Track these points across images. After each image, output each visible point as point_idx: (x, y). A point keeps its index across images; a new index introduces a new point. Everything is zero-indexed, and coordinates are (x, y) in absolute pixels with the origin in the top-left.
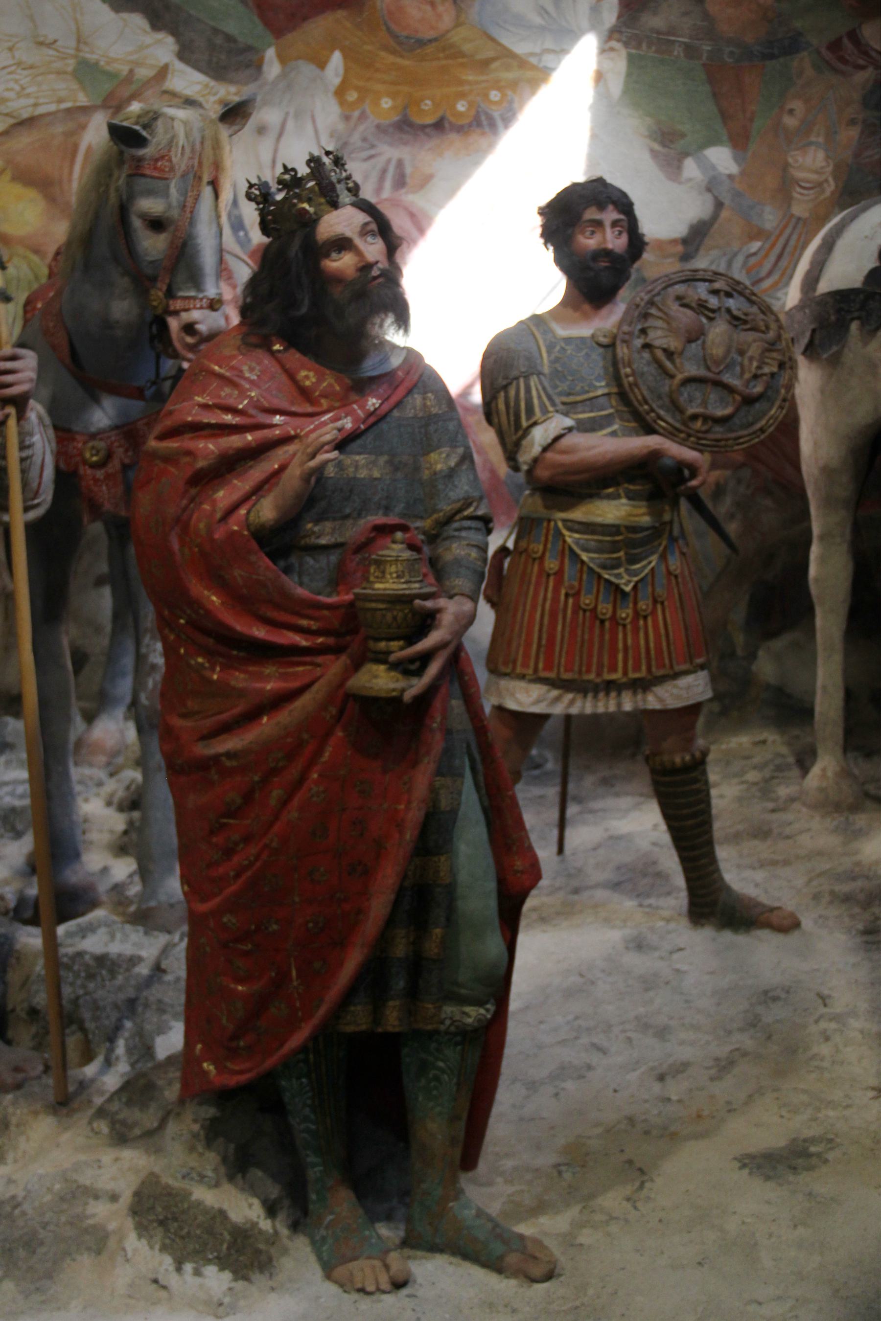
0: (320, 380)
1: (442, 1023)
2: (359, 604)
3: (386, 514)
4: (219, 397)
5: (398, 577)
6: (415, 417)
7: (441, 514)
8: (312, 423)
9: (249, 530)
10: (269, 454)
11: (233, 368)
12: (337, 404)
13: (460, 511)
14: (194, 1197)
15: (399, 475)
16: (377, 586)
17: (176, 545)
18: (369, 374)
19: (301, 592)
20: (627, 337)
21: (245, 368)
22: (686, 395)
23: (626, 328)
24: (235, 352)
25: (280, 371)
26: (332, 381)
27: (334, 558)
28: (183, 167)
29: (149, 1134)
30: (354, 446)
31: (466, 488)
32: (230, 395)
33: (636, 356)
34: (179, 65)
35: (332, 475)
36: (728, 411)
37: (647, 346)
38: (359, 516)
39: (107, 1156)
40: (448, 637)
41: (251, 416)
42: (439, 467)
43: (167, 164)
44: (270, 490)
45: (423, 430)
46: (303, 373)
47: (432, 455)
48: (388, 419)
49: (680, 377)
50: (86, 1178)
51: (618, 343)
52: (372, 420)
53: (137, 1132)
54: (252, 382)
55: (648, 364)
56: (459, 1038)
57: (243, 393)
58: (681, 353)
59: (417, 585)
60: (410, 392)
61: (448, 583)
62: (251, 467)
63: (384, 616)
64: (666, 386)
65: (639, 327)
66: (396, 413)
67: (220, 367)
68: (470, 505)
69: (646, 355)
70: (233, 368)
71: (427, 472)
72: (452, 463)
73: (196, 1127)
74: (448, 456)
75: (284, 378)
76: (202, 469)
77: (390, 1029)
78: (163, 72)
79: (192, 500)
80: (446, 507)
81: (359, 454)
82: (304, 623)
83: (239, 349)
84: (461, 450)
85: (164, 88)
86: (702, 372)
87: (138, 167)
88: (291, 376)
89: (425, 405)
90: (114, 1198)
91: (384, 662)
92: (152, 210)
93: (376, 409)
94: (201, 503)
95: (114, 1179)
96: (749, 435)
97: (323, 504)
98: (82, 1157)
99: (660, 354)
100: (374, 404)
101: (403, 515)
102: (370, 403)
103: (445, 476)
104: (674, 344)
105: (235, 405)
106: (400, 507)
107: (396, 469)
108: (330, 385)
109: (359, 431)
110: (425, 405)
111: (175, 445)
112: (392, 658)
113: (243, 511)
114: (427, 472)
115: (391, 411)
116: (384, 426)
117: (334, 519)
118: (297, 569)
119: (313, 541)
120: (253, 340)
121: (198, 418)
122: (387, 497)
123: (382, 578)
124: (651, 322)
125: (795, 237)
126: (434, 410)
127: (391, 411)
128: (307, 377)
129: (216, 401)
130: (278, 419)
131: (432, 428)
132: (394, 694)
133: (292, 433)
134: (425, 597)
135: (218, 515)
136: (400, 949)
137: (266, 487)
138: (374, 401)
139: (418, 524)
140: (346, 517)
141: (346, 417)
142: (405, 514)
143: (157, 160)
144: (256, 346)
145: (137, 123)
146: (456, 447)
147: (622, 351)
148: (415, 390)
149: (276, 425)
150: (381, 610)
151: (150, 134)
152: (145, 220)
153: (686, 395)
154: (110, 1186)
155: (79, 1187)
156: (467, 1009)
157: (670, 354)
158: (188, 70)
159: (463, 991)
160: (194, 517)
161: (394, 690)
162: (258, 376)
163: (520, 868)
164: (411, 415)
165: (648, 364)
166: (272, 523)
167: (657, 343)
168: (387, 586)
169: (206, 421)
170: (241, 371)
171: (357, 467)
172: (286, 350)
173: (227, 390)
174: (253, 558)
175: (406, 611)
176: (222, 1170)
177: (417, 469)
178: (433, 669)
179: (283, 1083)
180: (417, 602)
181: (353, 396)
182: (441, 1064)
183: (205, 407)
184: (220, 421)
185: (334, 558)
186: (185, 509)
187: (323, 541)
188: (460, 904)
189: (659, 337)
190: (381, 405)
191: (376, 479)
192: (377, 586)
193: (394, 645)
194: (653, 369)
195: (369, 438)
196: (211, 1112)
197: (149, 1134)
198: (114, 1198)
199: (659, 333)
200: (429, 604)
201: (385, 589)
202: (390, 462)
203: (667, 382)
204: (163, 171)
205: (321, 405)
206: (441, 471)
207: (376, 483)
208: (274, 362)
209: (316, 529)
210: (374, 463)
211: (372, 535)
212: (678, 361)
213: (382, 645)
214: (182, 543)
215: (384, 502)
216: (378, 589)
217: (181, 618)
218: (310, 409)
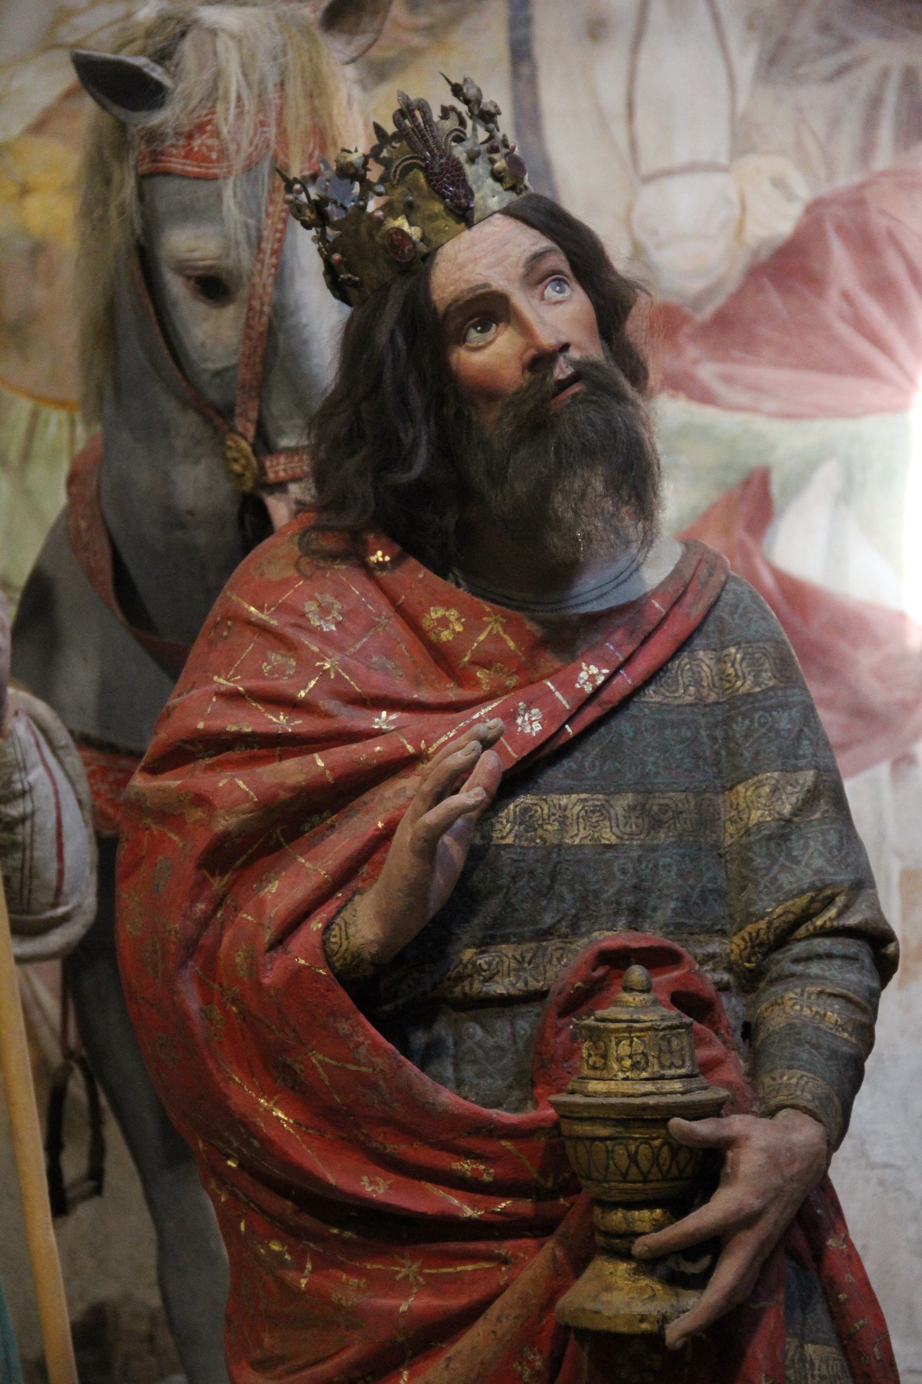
0: (471, 629)
2: (565, 1126)
3: (633, 926)
4: (259, 673)
5: (635, 1066)
6: (699, 703)
8: (454, 724)
9: (330, 965)
10: (366, 797)
11: (284, 609)
12: (511, 682)
13: (806, 916)
16: (594, 1086)
17: (193, 1003)
18: (583, 610)
19: (447, 1097)
21: (310, 607)
24: (291, 573)
25: (386, 610)
26: (498, 628)
27: (524, 1026)
28: (246, 149)
30: (556, 774)
32: (280, 670)
35: (509, 840)
38: (575, 929)
41: (326, 715)
42: (756, 815)
43: (211, 142)
44: (373, 878)
45: (719, 733)
46: (436, 613)
47: (740, 788)
48: (633, 710)
52: (591, 713)
54: (325, 638)
57: (307, 665)
59: (677, 1086)
60: (684, 645)
61: (767, 1081)
62: (332, 827)
63: (610, 1153)
66: (652, 695)
67: (260, 608)
68: (831, 900)
70: (284, 609)
71: (731, 829)
72: (787, 810)
74: (775, 790)
75: (395, 627)
76: (226, 835)
79: (219, 902)
81: (569, 791)
82: (465, 1167)
83: (297, 565)
84: (808, 777)
87: (155, 156)
89: (723, 676)
91: (627, 1256)
92: (197, 254)
93: (598, 690)
94: (237, 909)
97: (493, 905)
100: (592, 678)
101: (676, 928)
102: (583, 675)
103: (769, 838)
105: (291, 691)
107: (656, 824)
108: (495, 638)
109: (562, 741)
110: (723, 676)
111: (174, 783)
112: (639, 1246)
113: (316, 925)
114: (731, 829)
115: (638, 690)
116: (623, 725)
117: (521, 939)
118: (452, 1052)
119: (477, 987)
120: (329, 544)
121: (217, 724)
122: (635, 887)
123: (601, 1070)
126: (745, 686)
127: (638, 690)
128: (444, 622)
129: (253, 683)
131: (739, 727)
133: (410, 748)
134: (715, 1110)
135: (268, 936)
137: (365, 869)
138: (594, 670)
139: (714, 947)
140: (547, 934)
141: (528, 709)
142: (679, 926)
143: (190, 136)
144: (334, 557)
145: (142, 52)
146: (797, 769)
148: (698, 641)
149: (380, 733)
150: (603, 1139)
151: (173, 76)
152: (189, 278)
160: (226, 941)
162: (338, 624)
164: (689, 699)
166: (374, 949)
168: (612, 1086)
169: (232, 728)
170: (303, 615)
171: (563, 821)
172: (396, 562)
173: (276, 658)
174: (344, 1027)
175: (657, 1143)
180: (677, 1122)
181: (549, 661)
183: (232, 696)
184: (261, 729)
185: (524, 1026)
186: (206, 921)
187: (499, 988)
190: (609, 679)
191: (608, 847)
192: (594, 1086)
193: (643, 1217)
195: (592, 750)
200: (704, 1128)
201: (608, 1094)
202: (639, 809)
204: (207, 159)
205: (477, 683)
206: (759, 825)
207: (608, 855)
208: (373, 592)
209: (482, 961)
210: (602, 810)
211: (600, 972)
213: (617, 1217)
214: (207, 997)
215: (629, 899)
216: (595, 1094)
217: (228, 1157)
218: (453, 693)
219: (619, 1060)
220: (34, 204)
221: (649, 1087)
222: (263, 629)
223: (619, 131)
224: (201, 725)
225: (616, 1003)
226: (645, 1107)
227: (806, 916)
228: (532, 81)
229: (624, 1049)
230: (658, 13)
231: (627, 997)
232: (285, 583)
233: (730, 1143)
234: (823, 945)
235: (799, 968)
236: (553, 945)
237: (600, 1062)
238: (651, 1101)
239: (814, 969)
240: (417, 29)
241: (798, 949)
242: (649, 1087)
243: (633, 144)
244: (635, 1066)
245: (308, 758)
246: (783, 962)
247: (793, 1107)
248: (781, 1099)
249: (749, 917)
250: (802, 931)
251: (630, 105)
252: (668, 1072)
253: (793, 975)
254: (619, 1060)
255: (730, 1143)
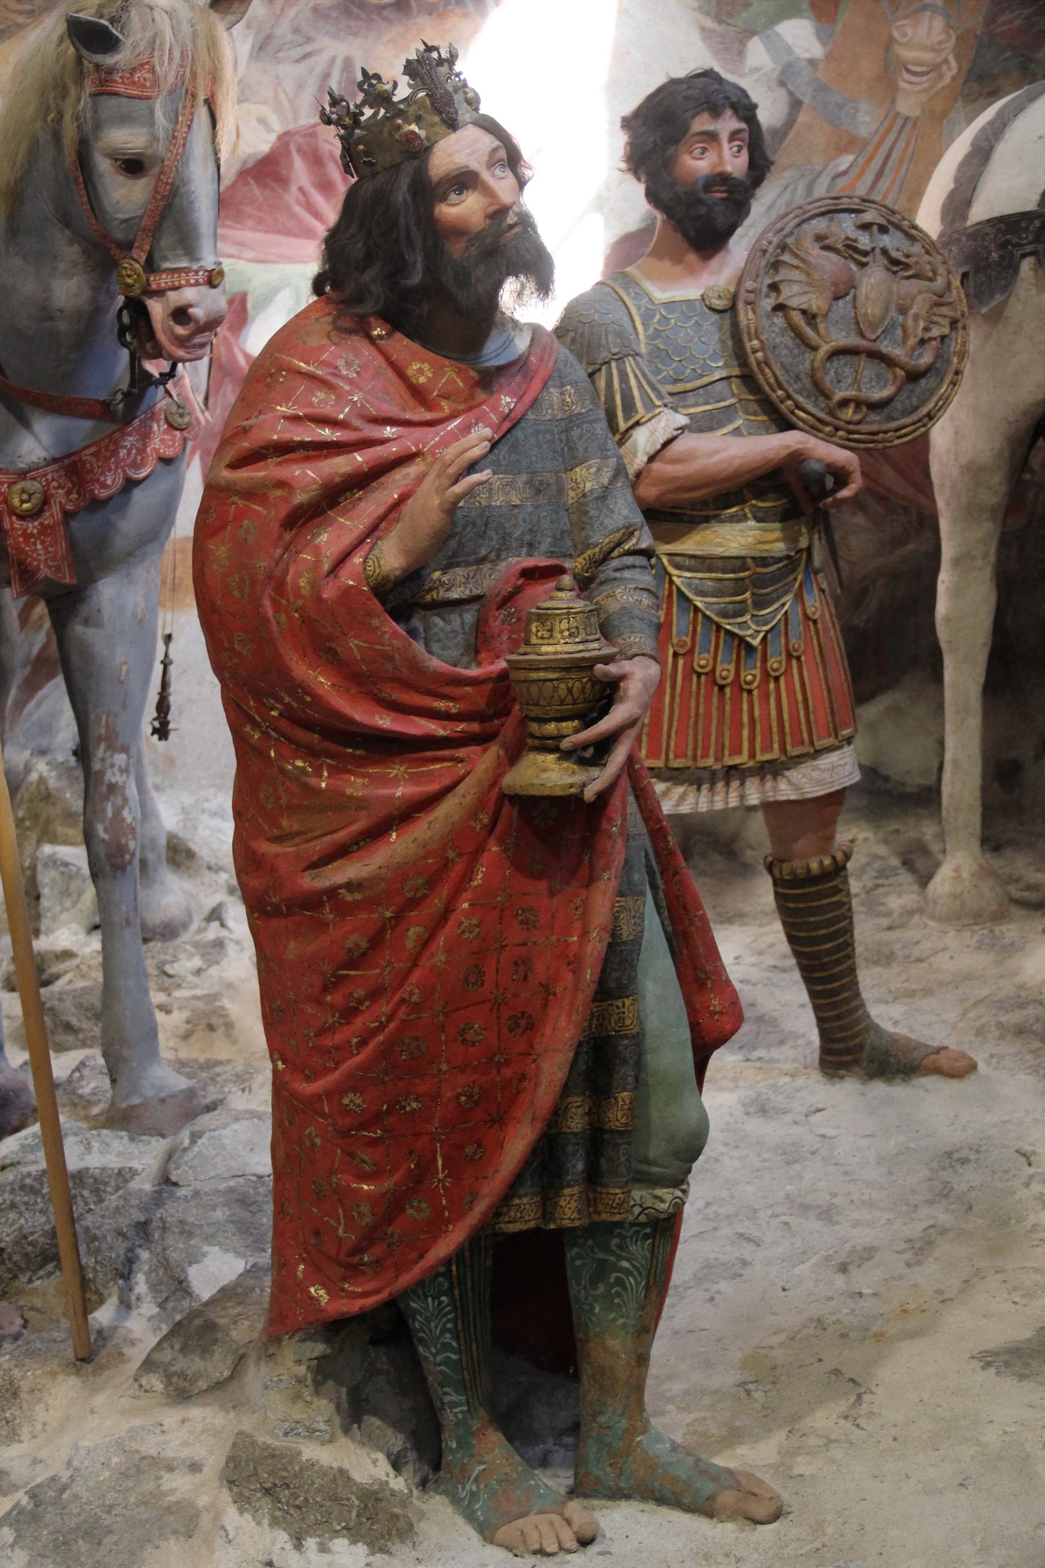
1: (630, 1211)
4: (311, 404)
7: (597, 550)
8: (438, 434)
11: (324, 364)
13: (619, 544)
14: (304, 1458)
15: (542, 500)
20: (752, 296)
21: (341, 363)
22: (832, 373)
23: (749, 284)
25: (384, 365)
29: (219, 1385)
31: (625, 512)
33: (765, 322)
36: (886, 393)
37: (780, 308)
39: (171, 1417)
40: (637, 711)
42: (588, 486)
47: (577, 469)
49: (825, 349)
50: (150, 1446)
51: (741, 305)
53: (203, 1384)
54: (350, 382)
55: (782, 333)
56: (648, 1230)
57: (341, 397)
58: (825, 316)
64: (805, 362)
65: (769, 281)
67: (307, 363)
68: (632, 534)
69: (779, 320)
70: (324, 364)
71: (572, 494)
72: (605, 481)
73: (302, 1370)
77: (567, 1223)
80: (601, 539)
86: (852, 340)
88: (400, 373)
90: (195, 1467)
95: (186, 1444)
96: (914, 423)
98: (137, 1422)
99: (797, 318)
103: (598, 498)
104: (816, 302)
105: (333, 415)
106: (545, 544)
107: (538, 492)
114: (572, 494)
116: (518, 433)
122: (531, 530)
124: (783, 274)
125: (901, 145)
129: (308, 411)
130: (389, 431)
132: (572, 790)
133: (414, 449)
136: (576, 1122)
142: (552, 552)
146: (607, 457)
147: (746, 317)
153: (832, 373)
154: (185, 1453)
155: (143, 1458)
156: (660, 1192)
157: (810, 317)
159: (654, 1170)
161: (572, 786)
162: (358, 373)
163: (718, 1009)
165: (782, 333)
167: (794, 302)
169: (297, 439)
170: (336, 368)
173: (321, 395)
176: (337, 1420)
177: (560, 490)
178: (619, 756)
179: (414, 1305)
182: (625, 1264)
183: (295, 419)
184: (317, 439)
188: (649, 1058)
189: (795, 295)
191: (515, 506)
194: (788, 339)
196: (320, 1348)
197: (219, 1385)
198: (195, 1467)
199: (796, 288)
202: (530, 483)
203: (808, 356)
205: (442, 409)
206: (592, 491)
207: (516, 511)
212: (822, 326)
215: (527, 538)
218: (428, 416)
219: (561, 632)
221: (581, 647)
222: (312, 377)
224: (275, 437)
225: (552, 599)
226: (583, 659)
227: (619, 544)
229: (564, 625)
231: (560, 594)
232: (321, 349)
233: (623, 677)
234: (629, 560)
235: (617, 575)
236: (488, 566)
237: (546, 634)
238: (587, 655)
239: (627, 574)
241: (615, 563)
242: (581, 647)
244: (571, 635)
245: (350, 456)
246: (608, 570)
247: (643, 655)
248: (634, 650)
249: (588, 546)
250: (616, 553)
252: (590, 638)
253: (615, 579)
254: (561, 632)
255: (623, 677)
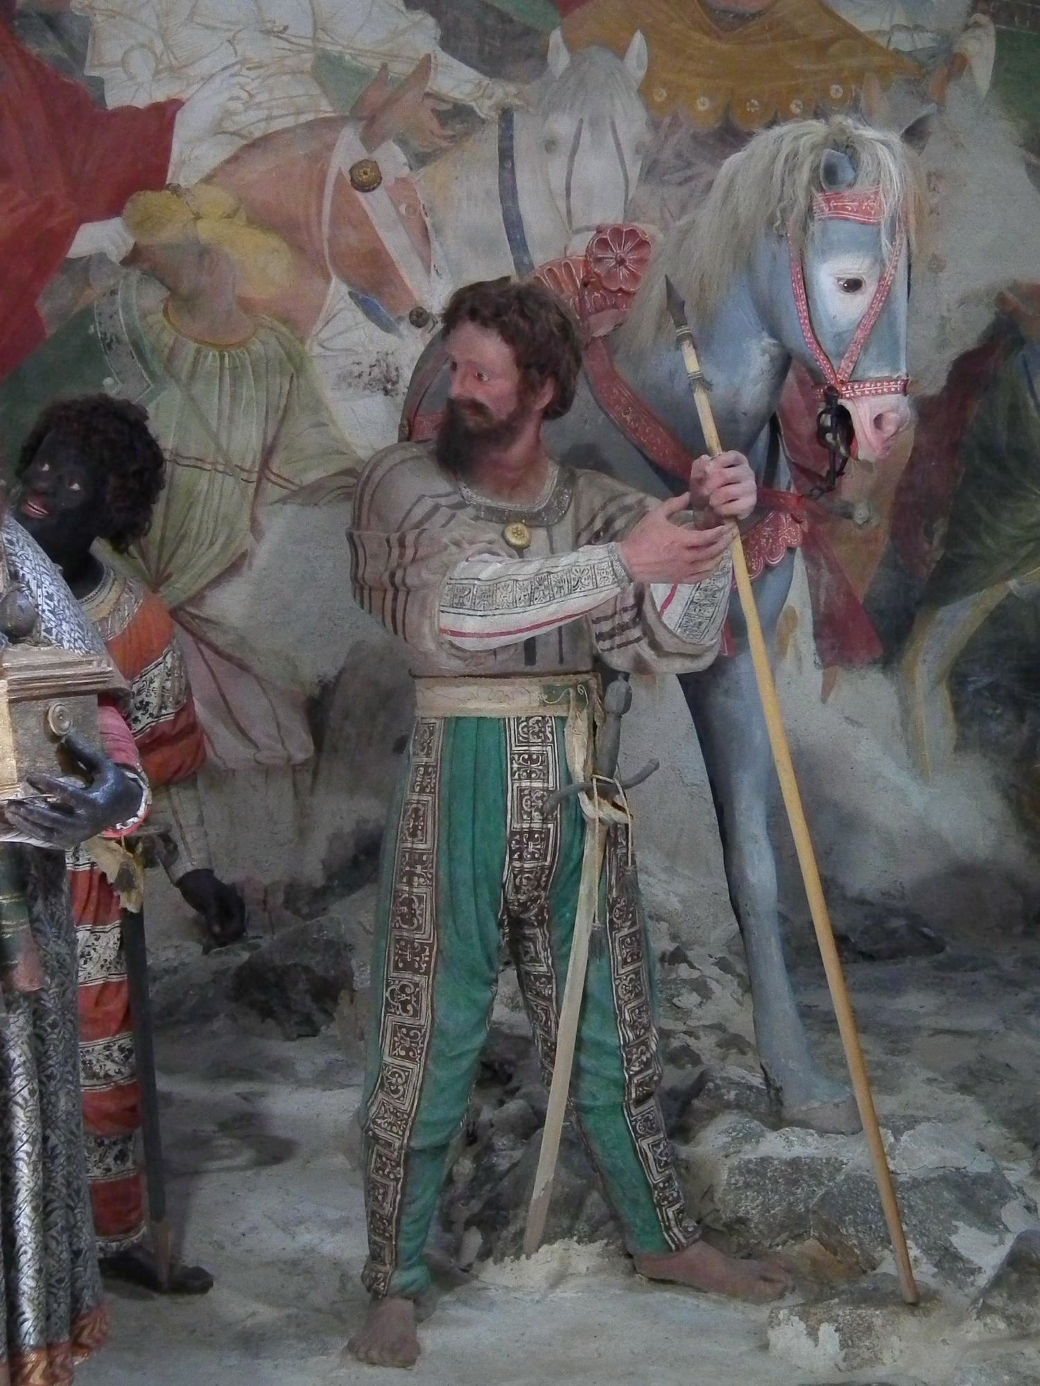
34: (444, 57)
78: (425, 67)
85: (427, 90)
158: (455, 63)
220: (200, 224)
223: (562, 205)
228: (513, 171)
230: (586, 135)
240: (445, 138)
243: (569, 212)
251: (568, 189)
